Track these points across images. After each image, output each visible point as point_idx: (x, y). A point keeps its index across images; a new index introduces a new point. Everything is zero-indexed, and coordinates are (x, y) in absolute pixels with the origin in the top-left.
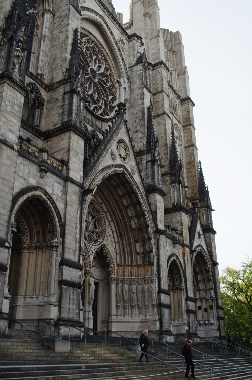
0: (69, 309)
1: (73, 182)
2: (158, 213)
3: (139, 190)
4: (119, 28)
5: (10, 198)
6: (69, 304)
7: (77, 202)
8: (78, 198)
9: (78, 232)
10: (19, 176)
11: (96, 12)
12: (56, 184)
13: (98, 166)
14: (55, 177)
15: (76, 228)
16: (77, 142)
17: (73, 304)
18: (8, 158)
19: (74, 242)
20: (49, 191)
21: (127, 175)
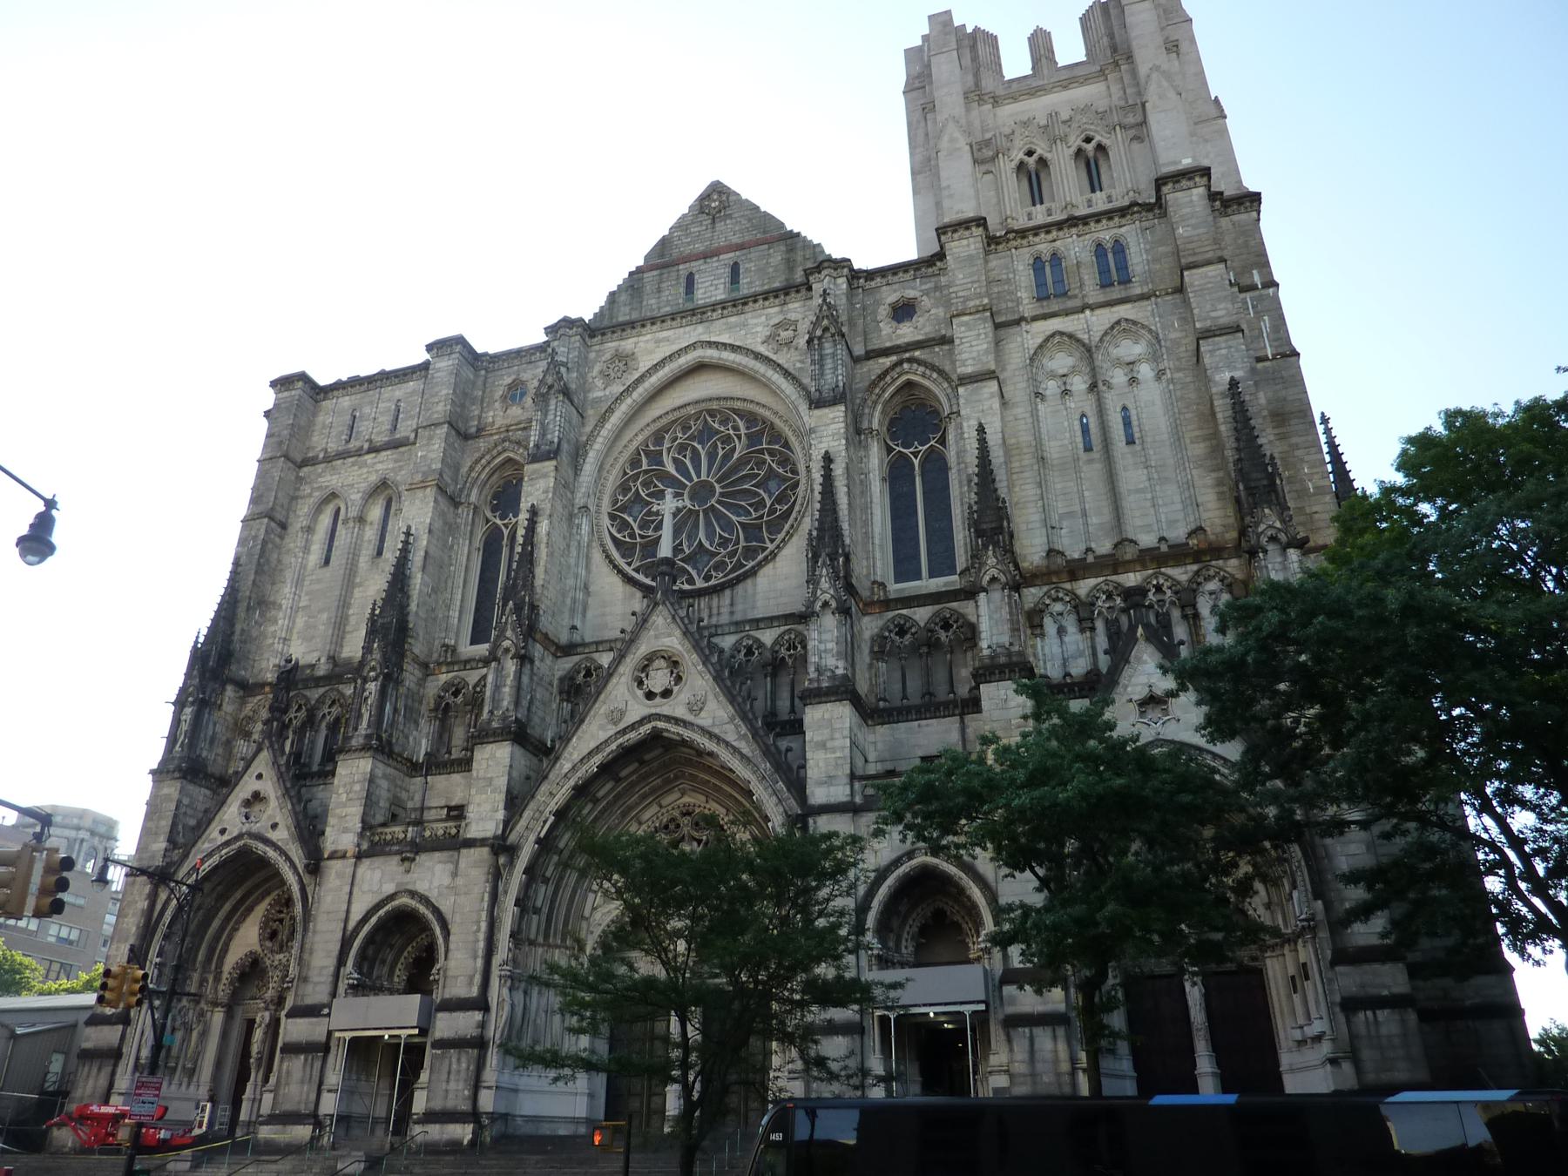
0: (447, 1091)
1: (471, 843)
2: (810, 763)
3: (718, 739)
4: (767, 303)
5: (340, 935)
6: (448, 1081)
7: (483, 878)
8: (486, 869)
9: (482, 936)
10: (364, 892)
11: (670, 356)
12: (439, 867)
13: (561, 767)
14: (437, 855)
15: (478, 930)
16: (493, 756)
17: (458, 1080)
18: (340, 875)
19: (471, 962)
20: (421, 887)
21: (667, 731)
